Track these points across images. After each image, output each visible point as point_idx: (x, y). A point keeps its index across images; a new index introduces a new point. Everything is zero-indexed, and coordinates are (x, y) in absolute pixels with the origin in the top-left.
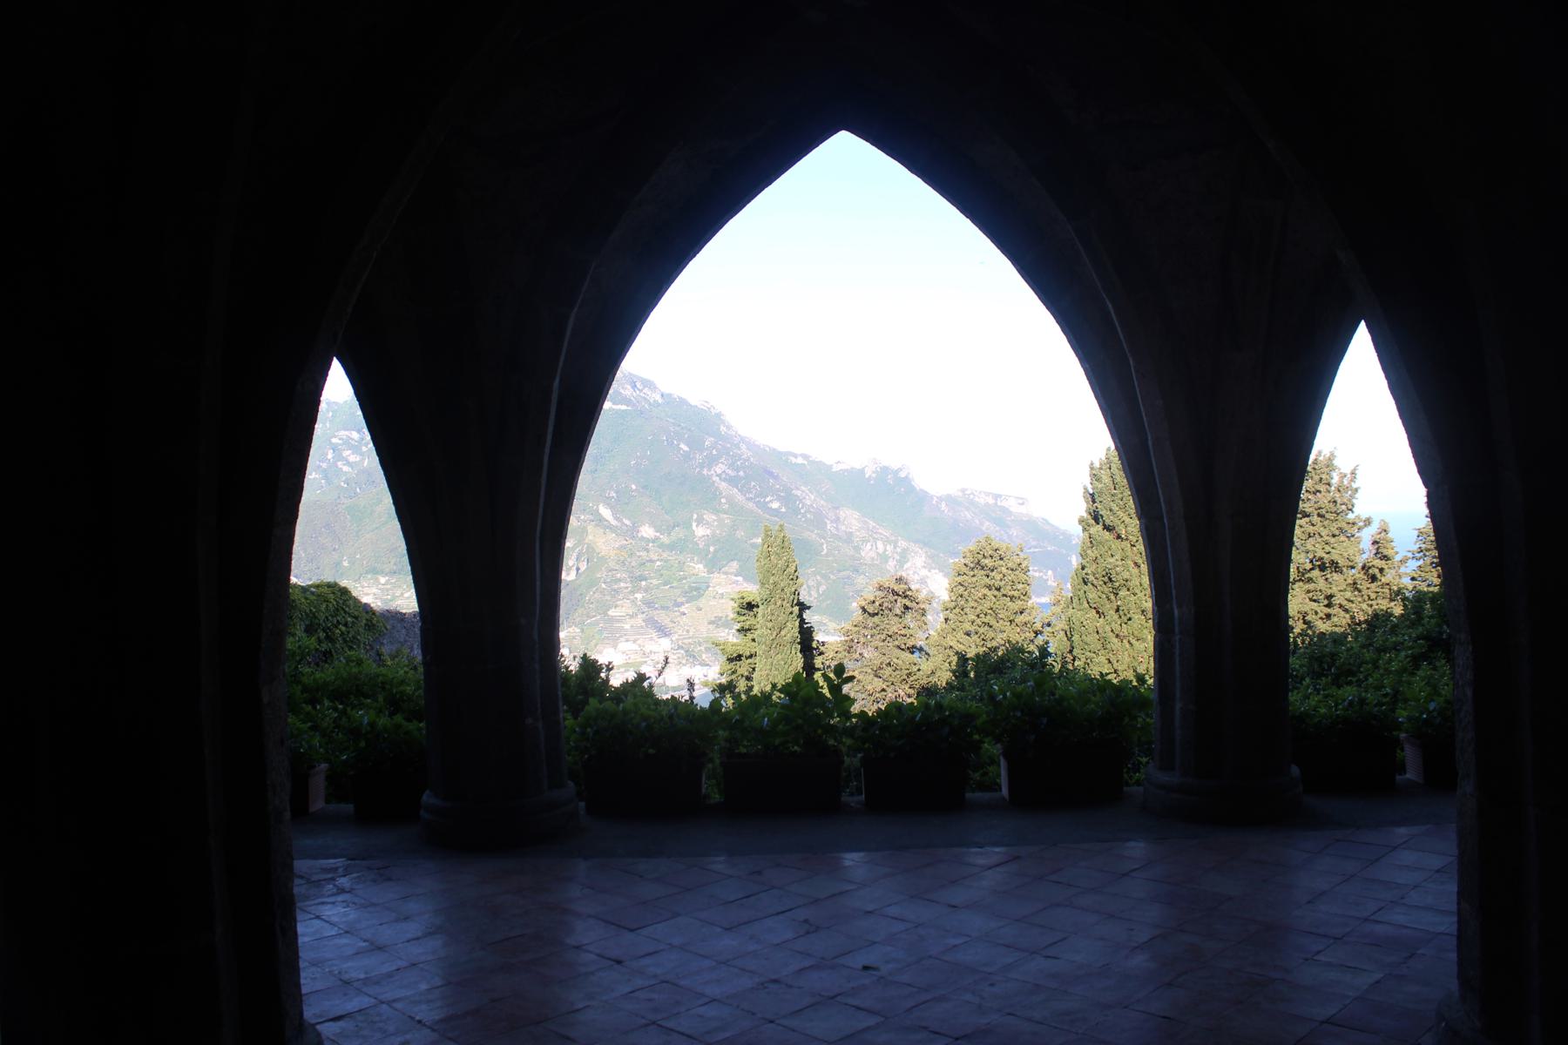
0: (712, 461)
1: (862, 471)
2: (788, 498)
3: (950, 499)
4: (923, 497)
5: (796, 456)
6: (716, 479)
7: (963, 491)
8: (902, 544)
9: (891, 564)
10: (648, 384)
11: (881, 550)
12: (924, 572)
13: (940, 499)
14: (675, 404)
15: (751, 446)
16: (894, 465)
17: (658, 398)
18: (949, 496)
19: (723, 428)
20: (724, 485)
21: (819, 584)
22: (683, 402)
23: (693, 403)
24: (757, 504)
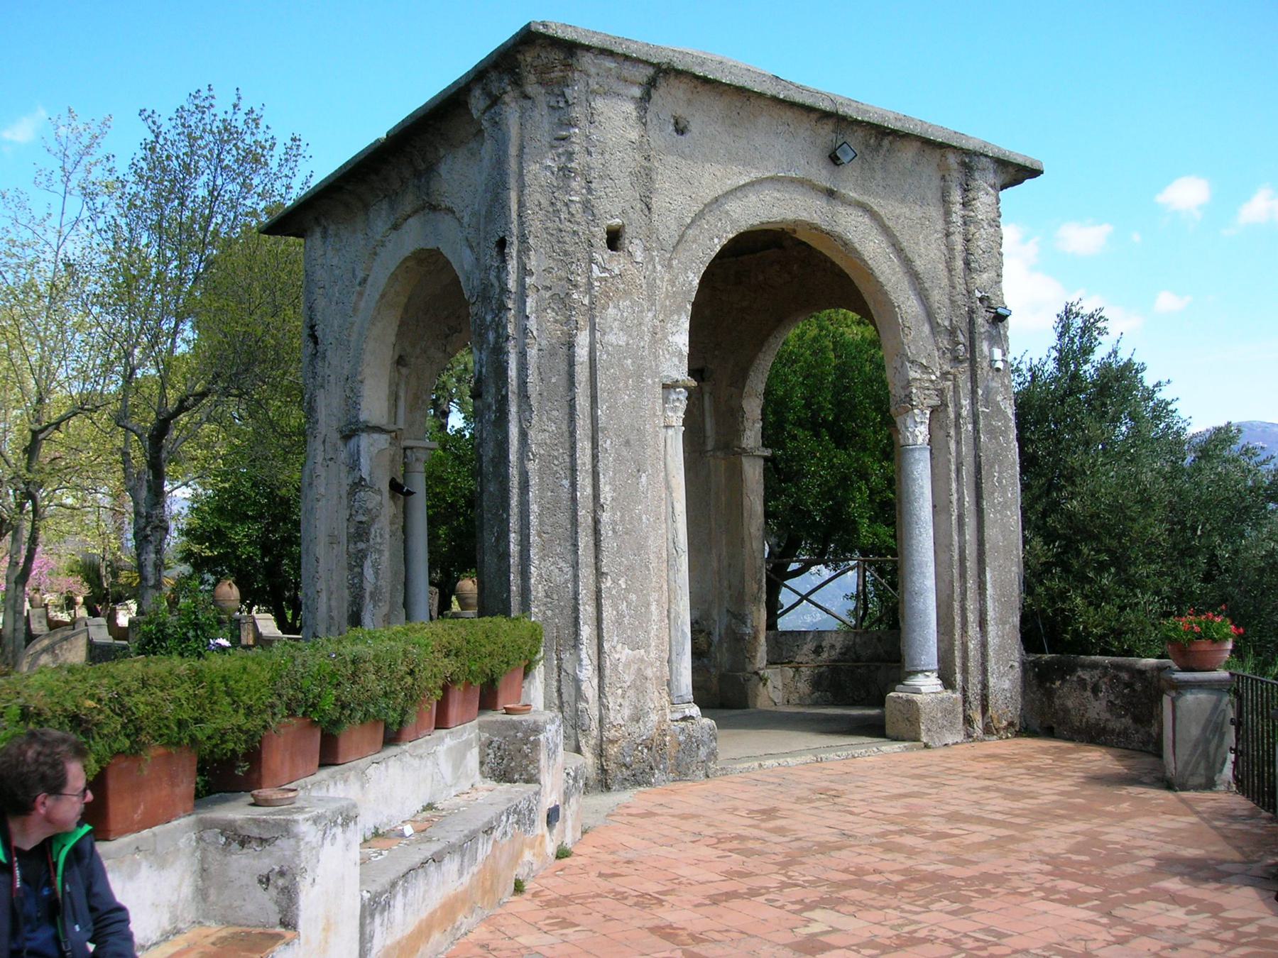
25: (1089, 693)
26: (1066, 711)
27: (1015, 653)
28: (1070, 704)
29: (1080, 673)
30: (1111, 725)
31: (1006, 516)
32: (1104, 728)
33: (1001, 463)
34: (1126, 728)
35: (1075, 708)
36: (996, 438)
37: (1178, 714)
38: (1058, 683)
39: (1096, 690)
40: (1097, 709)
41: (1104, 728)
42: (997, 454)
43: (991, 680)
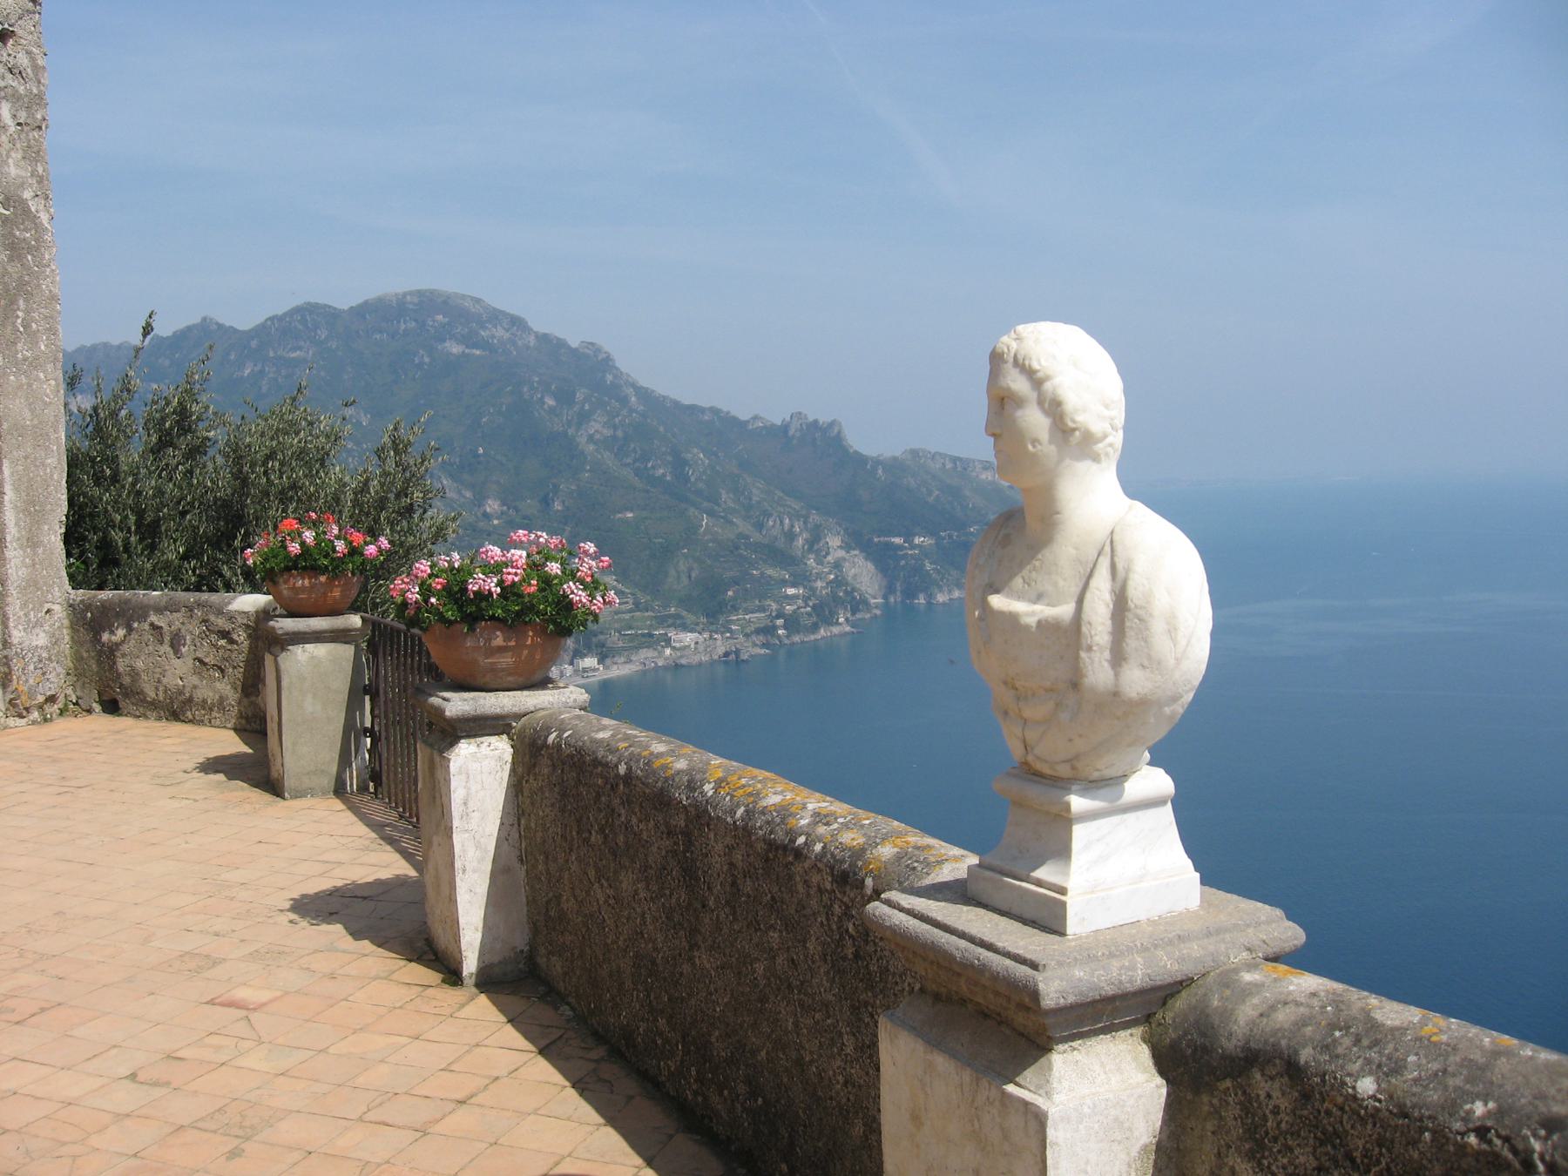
0: (584, 418)
1: (785, 428)
2: (679, 464)
3: (895, 466)
4: (860, 460)
5: (702, 410)
6: (583, 440)
7: (915, 453)
8: (815, 517)
9: (800, 542)
10: (517, 323)
11: (786, 527)
12: (841, 553)
13: (877, 462)
14: (552, 346)
15: (645, 394)
16: (824, 419)
17: (532, 341)
18: (895, 459)
19: (609, 378)
20: (592, 447)
21: (690, 569)
22: (561, 344)
23: (574, 343)
24: (637, 473)
25: (166, 648)
26: (134, 674)
27: (60, 592)
28: (140, 664)
29: (153, 618)
30: (199, 695)
31: (37, 379)
32: (190, 700)
33: (29, 296)
34: (222, 699)
35: (146, 671)
36: (20, 258)
37: (284, 683)
38: (121, 633)
39: (176, 642)
40: (178, 672)
41: (190, 700)
42: (22, 284)
43: (15, 633)
